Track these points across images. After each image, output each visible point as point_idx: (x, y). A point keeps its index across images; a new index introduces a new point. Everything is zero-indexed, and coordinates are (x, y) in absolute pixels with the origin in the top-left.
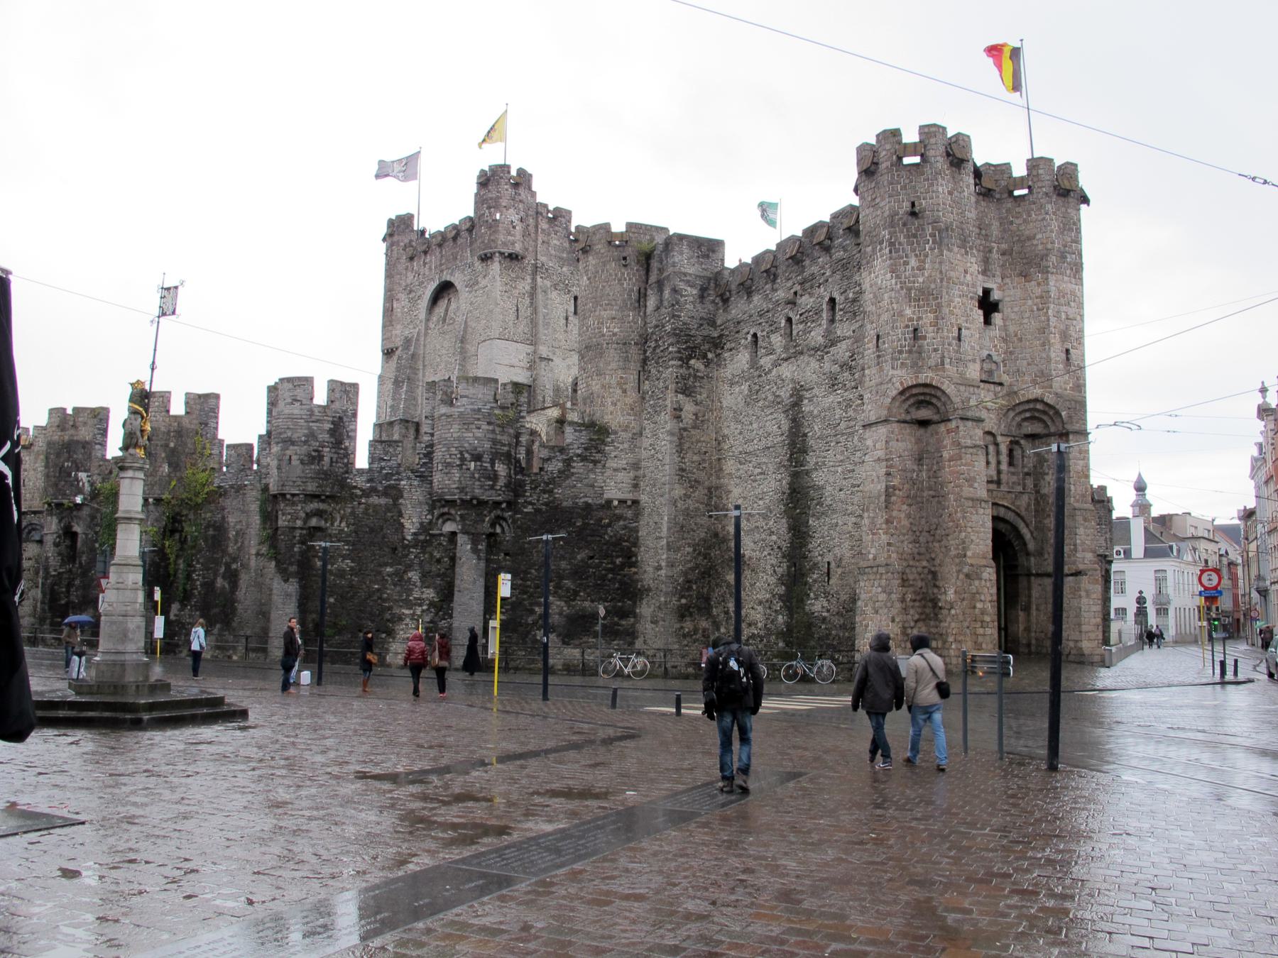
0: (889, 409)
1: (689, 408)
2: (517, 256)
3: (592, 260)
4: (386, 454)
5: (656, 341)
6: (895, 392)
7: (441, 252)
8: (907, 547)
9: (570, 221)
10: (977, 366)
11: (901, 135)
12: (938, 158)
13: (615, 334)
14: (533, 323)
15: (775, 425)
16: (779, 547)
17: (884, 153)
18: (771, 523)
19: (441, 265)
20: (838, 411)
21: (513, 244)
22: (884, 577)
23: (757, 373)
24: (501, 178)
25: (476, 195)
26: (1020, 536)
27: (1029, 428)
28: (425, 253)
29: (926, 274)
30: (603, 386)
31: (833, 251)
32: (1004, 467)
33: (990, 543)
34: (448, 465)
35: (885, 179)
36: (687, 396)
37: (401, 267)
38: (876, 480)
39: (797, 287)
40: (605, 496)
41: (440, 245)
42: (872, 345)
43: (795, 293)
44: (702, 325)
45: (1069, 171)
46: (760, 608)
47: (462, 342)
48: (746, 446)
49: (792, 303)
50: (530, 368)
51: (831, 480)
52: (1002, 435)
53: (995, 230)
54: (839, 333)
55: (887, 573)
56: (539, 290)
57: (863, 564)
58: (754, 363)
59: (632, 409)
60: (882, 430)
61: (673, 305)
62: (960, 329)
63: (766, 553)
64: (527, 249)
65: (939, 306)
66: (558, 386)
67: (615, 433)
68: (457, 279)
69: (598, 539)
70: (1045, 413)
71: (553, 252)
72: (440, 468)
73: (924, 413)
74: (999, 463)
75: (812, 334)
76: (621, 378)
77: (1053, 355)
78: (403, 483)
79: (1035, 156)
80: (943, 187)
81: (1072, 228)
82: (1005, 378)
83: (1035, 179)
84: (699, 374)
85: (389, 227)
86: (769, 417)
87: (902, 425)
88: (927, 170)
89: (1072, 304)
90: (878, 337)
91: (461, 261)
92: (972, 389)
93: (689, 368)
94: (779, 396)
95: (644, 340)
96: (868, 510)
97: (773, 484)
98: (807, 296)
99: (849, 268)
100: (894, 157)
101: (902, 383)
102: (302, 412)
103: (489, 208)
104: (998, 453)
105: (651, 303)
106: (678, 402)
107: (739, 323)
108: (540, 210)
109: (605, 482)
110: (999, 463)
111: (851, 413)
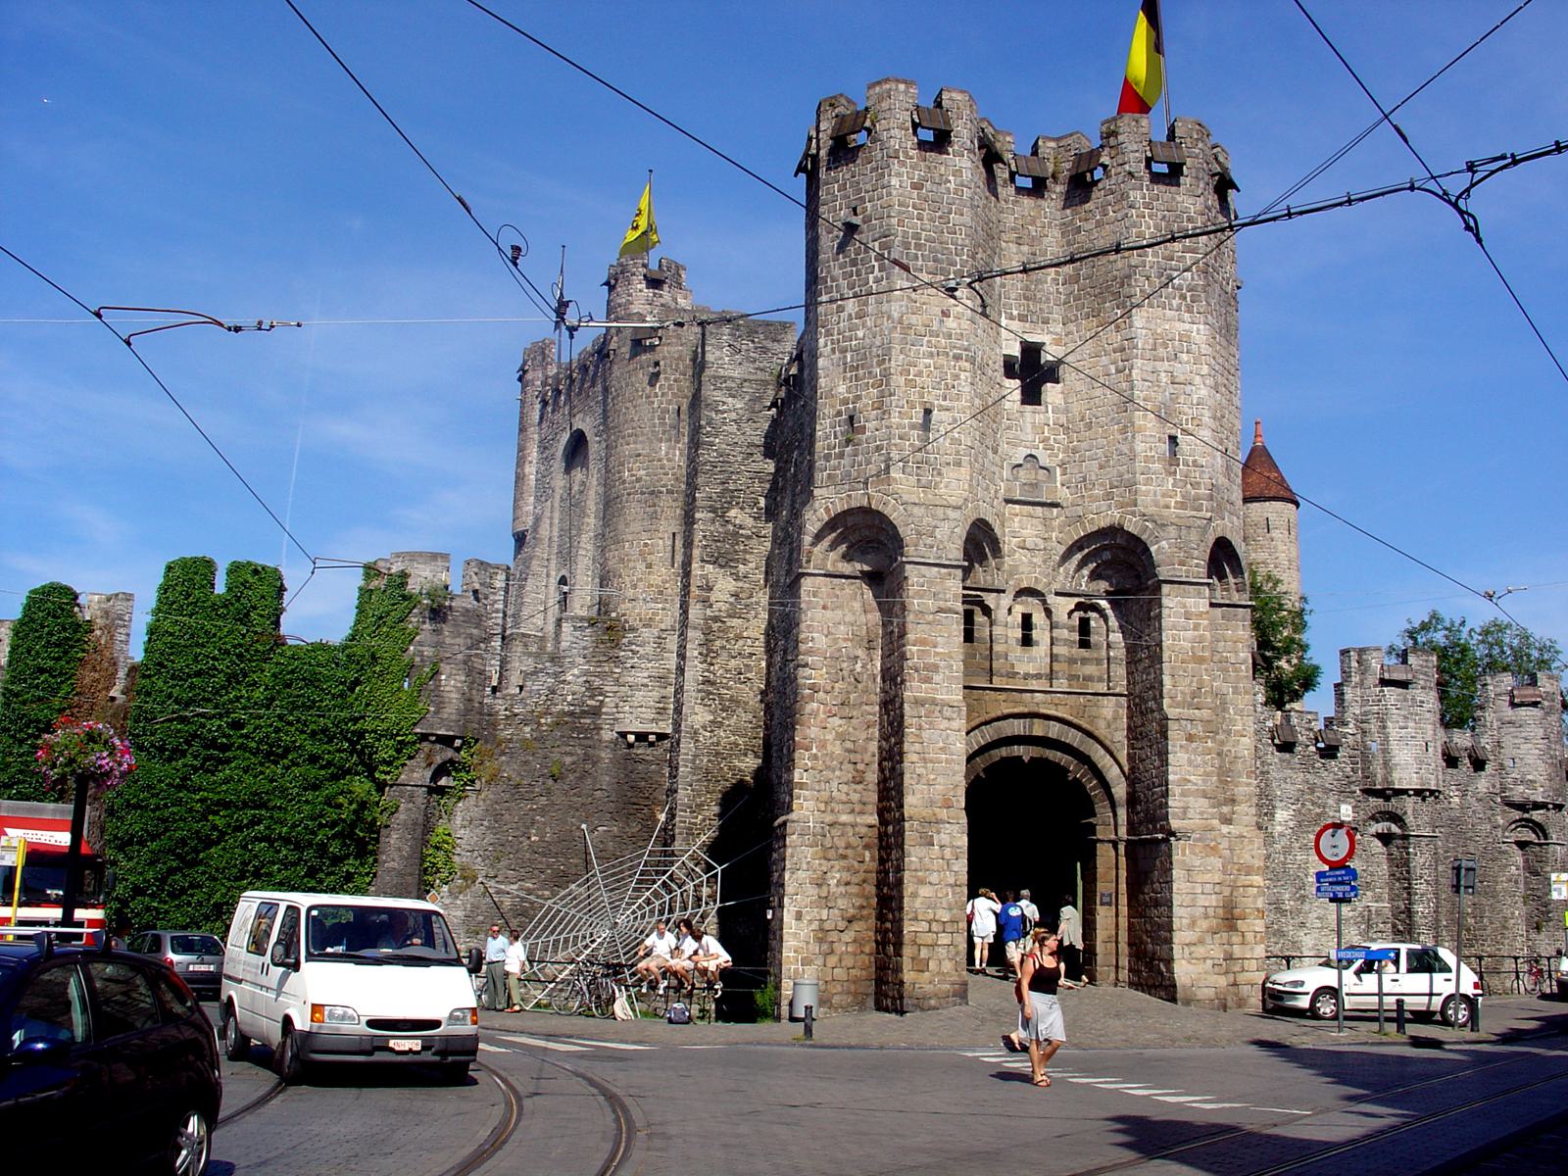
13: (639, 480)
24: (633, 274)
36: (721, 566)
59: (661, 593)
62: (928, 412)
65: (887, 375)
67: (633, 629)
76: (646, 545)
77: (1140, 447)
82: (1063, 494)
89: (1185, 357)
92: (940, 511)
101: (827, 510)
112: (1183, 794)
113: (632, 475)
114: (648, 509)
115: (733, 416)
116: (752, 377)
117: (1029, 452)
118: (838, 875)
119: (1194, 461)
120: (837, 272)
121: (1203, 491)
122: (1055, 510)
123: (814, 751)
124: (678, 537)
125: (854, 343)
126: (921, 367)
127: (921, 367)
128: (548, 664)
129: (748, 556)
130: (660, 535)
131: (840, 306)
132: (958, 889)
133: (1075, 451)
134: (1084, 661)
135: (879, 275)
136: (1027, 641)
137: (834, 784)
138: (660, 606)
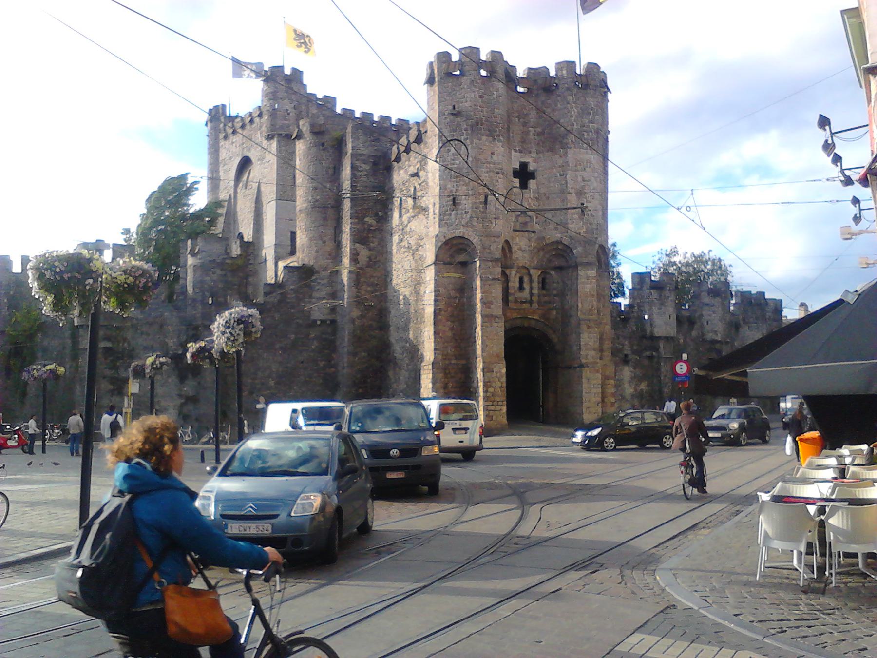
9: (335, 105)
13: (317, 201)
19: (243, 144)
27: (557, 262)
32: (535, 291)
36: (362, 244)
53: (533, 116)
59: (330, 255)
62: (486, 198)
67: (318, 272)
68: (253, 155)
73: (462, 258)
74: (531, 288)
78: (166, 314)
82: (537, 227)
84: (371, 228)
92: (493, 239)
93: (364, 224)
104: (531, 281)
110: (531, 288)
112: (586, 350)
115: (365, 173)
116: (374, 154)
121: (594, 226)
122: (533, 235)
134: (544, 296)
136: (521, 288)
137: (449, 348)
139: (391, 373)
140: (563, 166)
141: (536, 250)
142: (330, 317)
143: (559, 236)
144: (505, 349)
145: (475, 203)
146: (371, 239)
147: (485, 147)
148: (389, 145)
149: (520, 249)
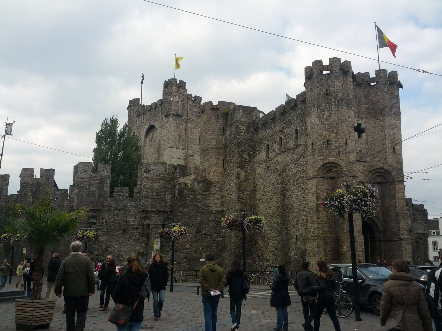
0: (317, 172)
1: (243, 174)
2: (180, 115)
3: (205, 116)
4: (122, 193)
5: (230, 147)
6: (320, 166)
7: (150, 114)
8: (326, 229)
9: (201, 101)
10: (355, 155)
11: (322, 62)
12: (337, 71)
13: (214, 145)
14: (186, 141)
15: (275, 179)
16: (277, 229)
17: (315, 70)
18: (275, 219)
19: (150, 118)
20: (299, 174)
21: (178, 110)
22: (317, 241)
23: (269, 159)
25: (163, 91)
26: (376, 225)
28: (144, 114)
29: (332, 118)
30: (209, 166)
31: (297, 110)
33: (361, 227)
34: (146, 197)
35: (315, 80)
36: (242, 169)
37: (134, 120)
38: (313, 201)
39: (284, 125)
40: (210, 209)
41: (150, 111)
42: (310, 147)
43: (283, 127)
44: (248, 141)
45: (394, 74)
46: (270, 254)
47: (158, 149)
48: (264, 189)
49: (281, 131)
50: (185, 159)
51: (297, 202)
52: (367, 183)
53: (363, 99)
54: (299, 143)
55: (318, 239)
56: (188, 129)
57: (308, 236)
58: (267, 155)
59: (221, 174)
60: (315, 181)
61: (236, 133)
62: (346, 140)
63: (272, 231)
64: (183, 112)
65: (338, 131)
66: (196, 166)
68: (156, 124)
69: (207, 226)
70: (385, 173)
71: (194, 113)
72: (143, 198)
73: (331, 175)
75: (289, 143)
76: (217, 162)
78: (128, 204)
79: (380, 69)
80: (338, 83)
81: (396, 98)
82: (367, 159)
83: (379, 78)
84: (246, 160)
85: (129, 104)
86: (273, 177)
87: (323, 179)
88: (332, 76)
89: (396, 129)
90: (313, 144)
91: (158, 117)
94: (277, 168)
95: (225, 148)
96: (310, 214)
97: (274, 204)
98: (287, 129)
99: (303, 117)
100: (319, 71)
101: (322, 162)
102: (87, 176)
103: (168, 96)
105: (228, 133)
106: (238, 171)
107: (262, 140)
108: (188, 97)
109: (210, 203)
111: (304, 175)
113: (212, 144)
114: (217, 153)
115: (243, 131)
116: (247, 121)
117: (360, 149)
118: (328, 249)
119: (399, 153)
120: (322, 105)
122: (365, 163)
123: (321, 219)
124: (224, 160)
125: (328, 122)
126: (344, 129)
127: (344, 129)
128: (191, 192)
129: (248, 167)
130: (220, 160)
131: (323, 113)
132: (363, 253)
133: (370, 149)
135: (335, 106)
137: (326, 227)
138: (221, 178)
139: (260, 242)
140: (382, 126)
141: (367, 173)
142: (220, 209)
143: (382, 165)
144: (362, 228)
145: (341, 143)
146: (246, 166)
147: (345, 113)
148: (255, 117)
149: (359, 171)
